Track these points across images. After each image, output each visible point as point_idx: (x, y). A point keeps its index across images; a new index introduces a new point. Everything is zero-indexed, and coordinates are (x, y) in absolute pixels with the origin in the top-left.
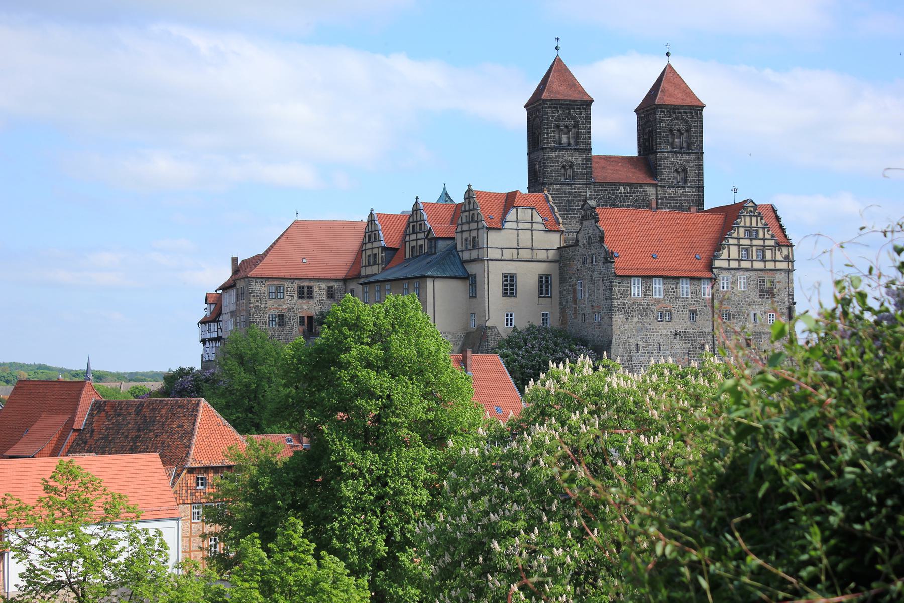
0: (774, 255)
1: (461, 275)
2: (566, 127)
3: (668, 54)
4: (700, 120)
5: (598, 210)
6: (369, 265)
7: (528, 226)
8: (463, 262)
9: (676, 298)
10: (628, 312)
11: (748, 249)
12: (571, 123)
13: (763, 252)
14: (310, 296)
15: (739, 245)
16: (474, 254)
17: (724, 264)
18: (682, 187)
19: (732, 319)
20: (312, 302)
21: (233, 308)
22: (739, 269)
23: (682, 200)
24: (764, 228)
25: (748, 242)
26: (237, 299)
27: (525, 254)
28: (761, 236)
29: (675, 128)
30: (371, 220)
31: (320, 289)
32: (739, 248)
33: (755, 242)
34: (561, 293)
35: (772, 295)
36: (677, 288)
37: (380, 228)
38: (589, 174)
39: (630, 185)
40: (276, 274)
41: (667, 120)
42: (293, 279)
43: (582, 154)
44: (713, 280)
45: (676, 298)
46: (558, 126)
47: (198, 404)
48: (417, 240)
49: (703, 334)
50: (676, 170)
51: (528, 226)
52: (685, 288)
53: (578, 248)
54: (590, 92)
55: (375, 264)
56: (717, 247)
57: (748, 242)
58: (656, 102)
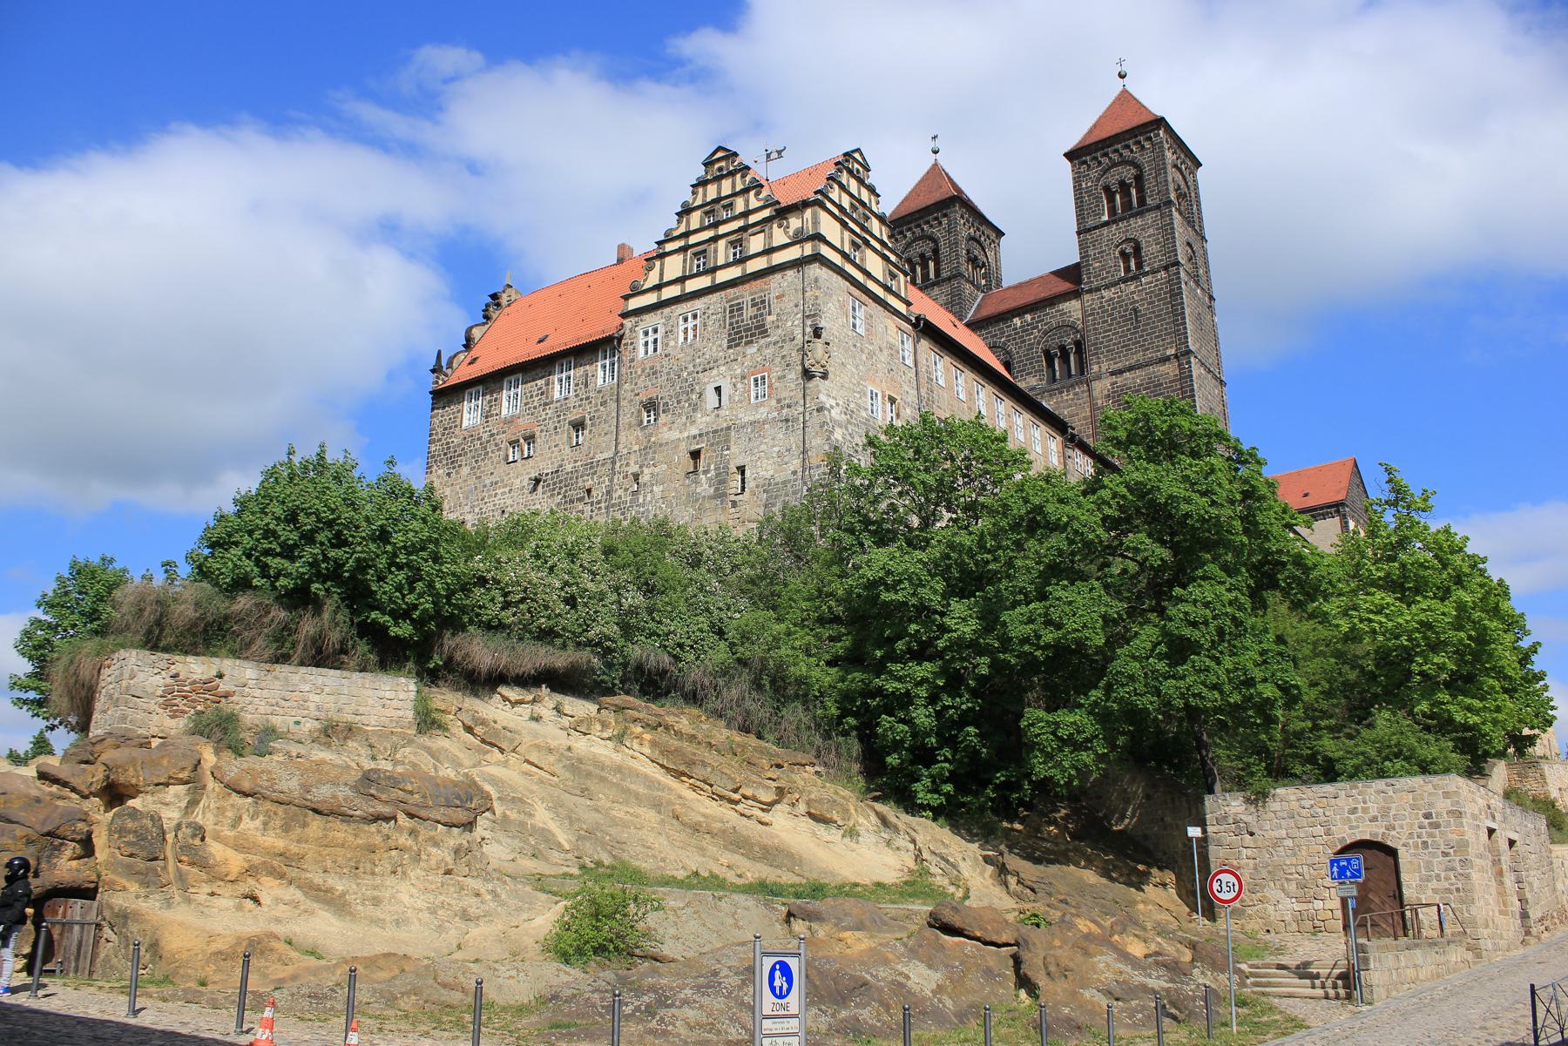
2: (922, 256)
9: (546, 404)
19: (663, 418)
23: (1137, 302)
32: (685, 256)
36: (547, 384)
45: (546, 404)
49: (591, 466)
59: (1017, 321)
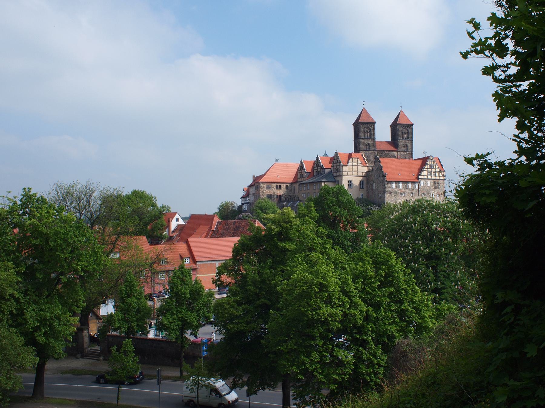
0: (439, 174)
1: (333, 180)
2: (367, 131)
3: (401, 107)
4: (412, 129)
5: (380, 159)
6: (300, 178)
7: (356, 164)
8: (334, 177)
10: (391, 193)
11: (430, 172)
12: (369, 130)
13: (435, 173)
14: (280, 188)
15: (427, 171)
16: (338, 174)
17: (423, 177)
18: (406, 152)
20: (281, 190)
21: (254, 192)
22: (427, 179)
24: (435, 165)
25: (430, 170)
26: (255, 189)
27: (355, 174)
28: (435, 168)
29: (404, 132)
30: (301, 163)
31: (283, 186)
33: (433, 170)
34: (367, 187)
35: (438, 188)
37: (304, 165)
38: (374, 147)
39: (389, 151)
40: (269, 181)
41: (401, 129)
42: (274, 183)
43: (373, 141)
44: (419, 183)
46: (364, 131)
47: (256, 221)
48: (318, 169)
50: (404, 146)
51: (356, 164)
52: (409, 186)
53: (373, 172)
54: (375, 120)
55: (302, 177)
56: (420, 171)
57: (430, 170)
58: (397, 123)
59: (386, 152)
